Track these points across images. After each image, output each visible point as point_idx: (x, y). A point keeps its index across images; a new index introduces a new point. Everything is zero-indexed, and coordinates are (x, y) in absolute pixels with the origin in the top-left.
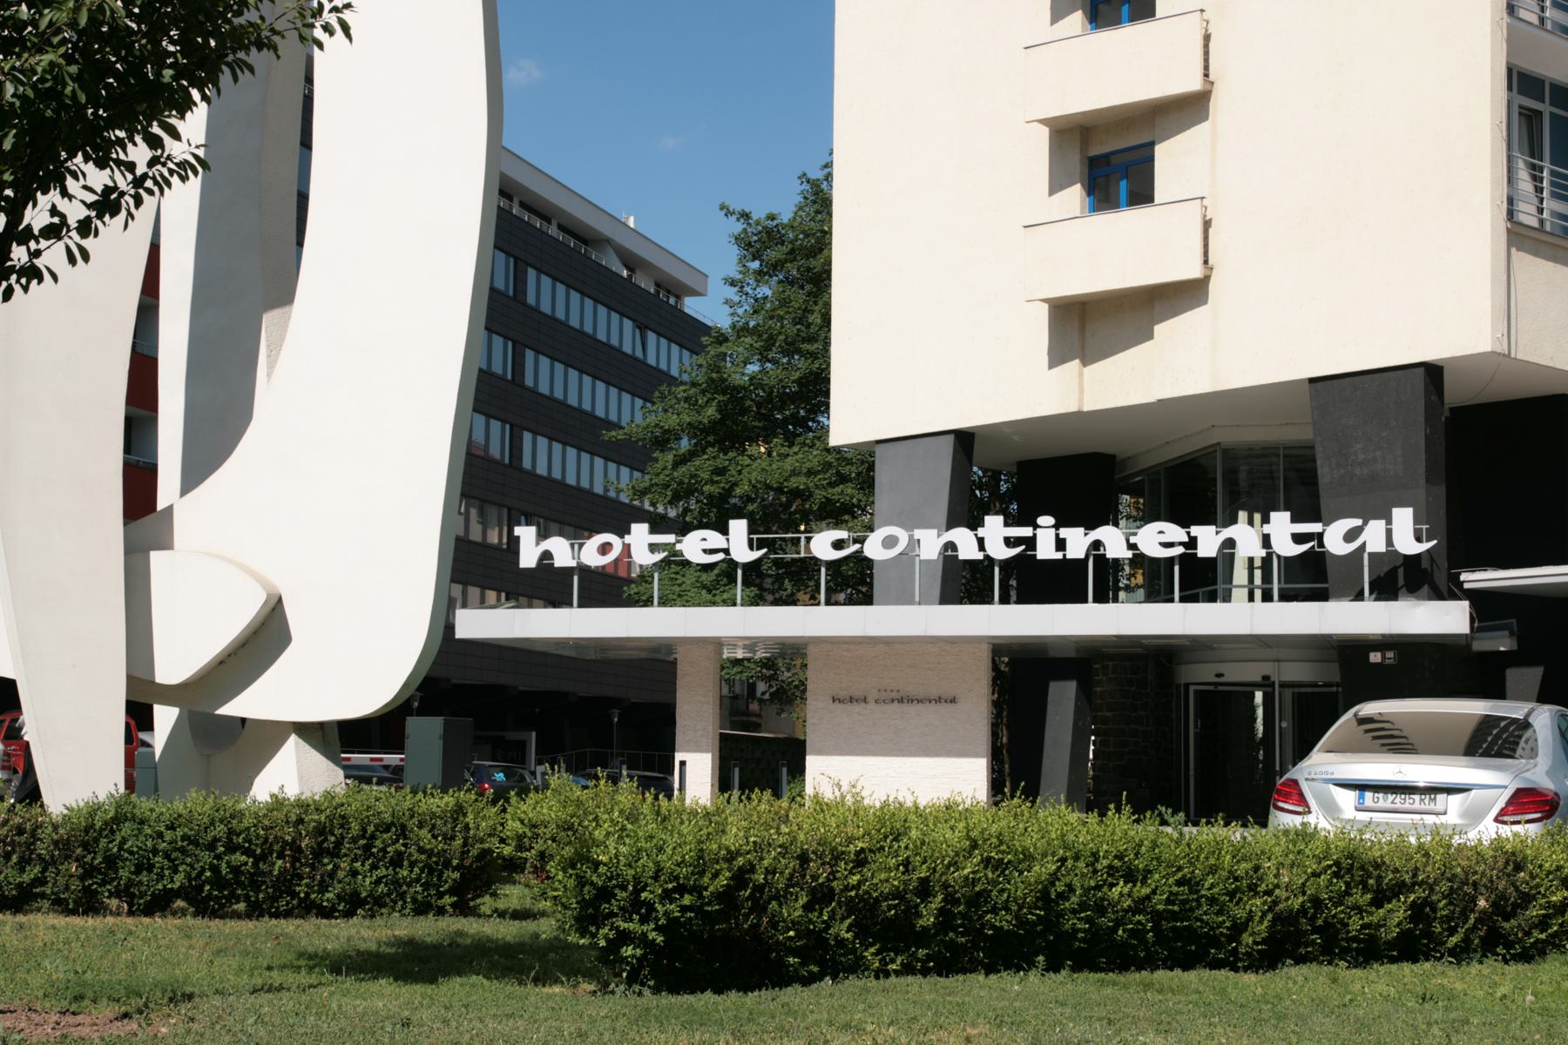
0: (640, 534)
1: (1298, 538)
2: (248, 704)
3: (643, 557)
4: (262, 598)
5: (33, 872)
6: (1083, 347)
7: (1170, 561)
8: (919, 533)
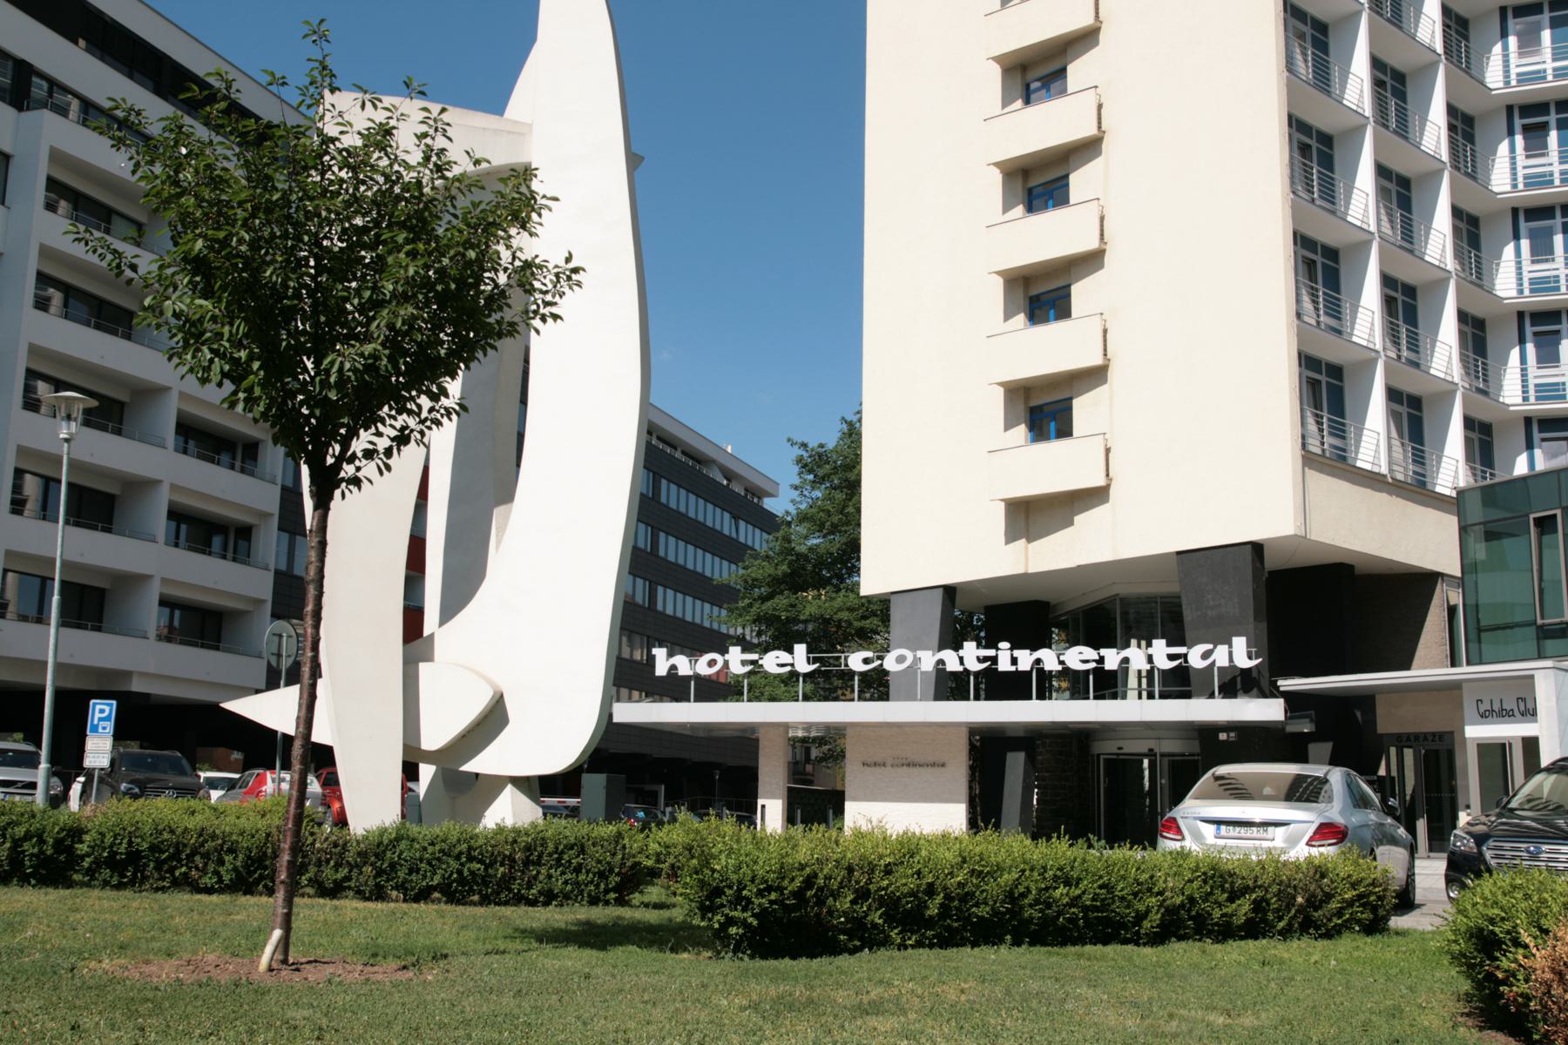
1: (1171, 657)
2: (482, 763)
3: (737, 669)
4: (492, 693)
6: (1028, 530)
7: (1087, 672)
8: (920, 654)
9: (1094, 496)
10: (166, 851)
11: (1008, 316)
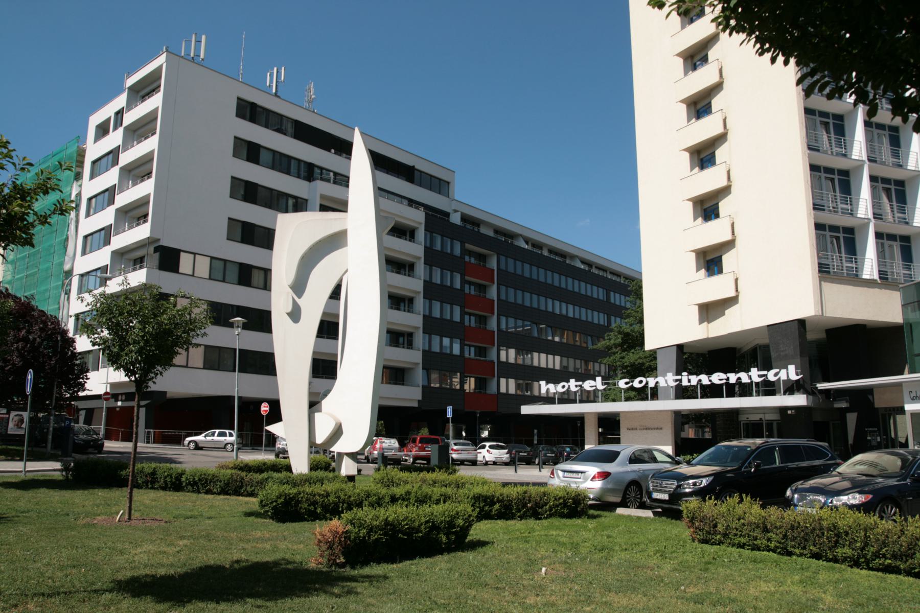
0: (572, 381)
1: (760, 376)
2: (337, 448)
4: (334, 424)
5: (253, 488)
7: (722, 385)
8: (648, 379)
9: (731, 301)
11: (695, 219)
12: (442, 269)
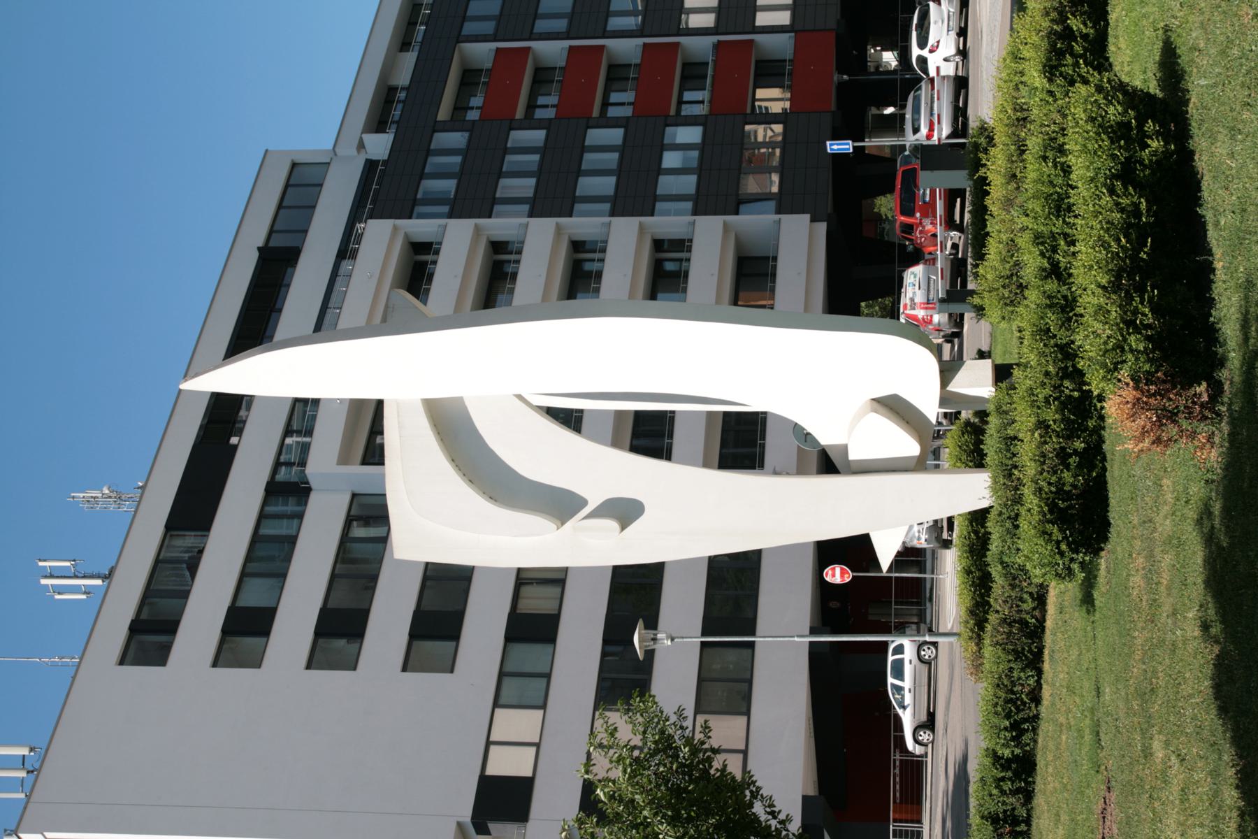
2: (931, 409)
5: (1026, 596)
10: (1010, 708)
12: (500, 175)
